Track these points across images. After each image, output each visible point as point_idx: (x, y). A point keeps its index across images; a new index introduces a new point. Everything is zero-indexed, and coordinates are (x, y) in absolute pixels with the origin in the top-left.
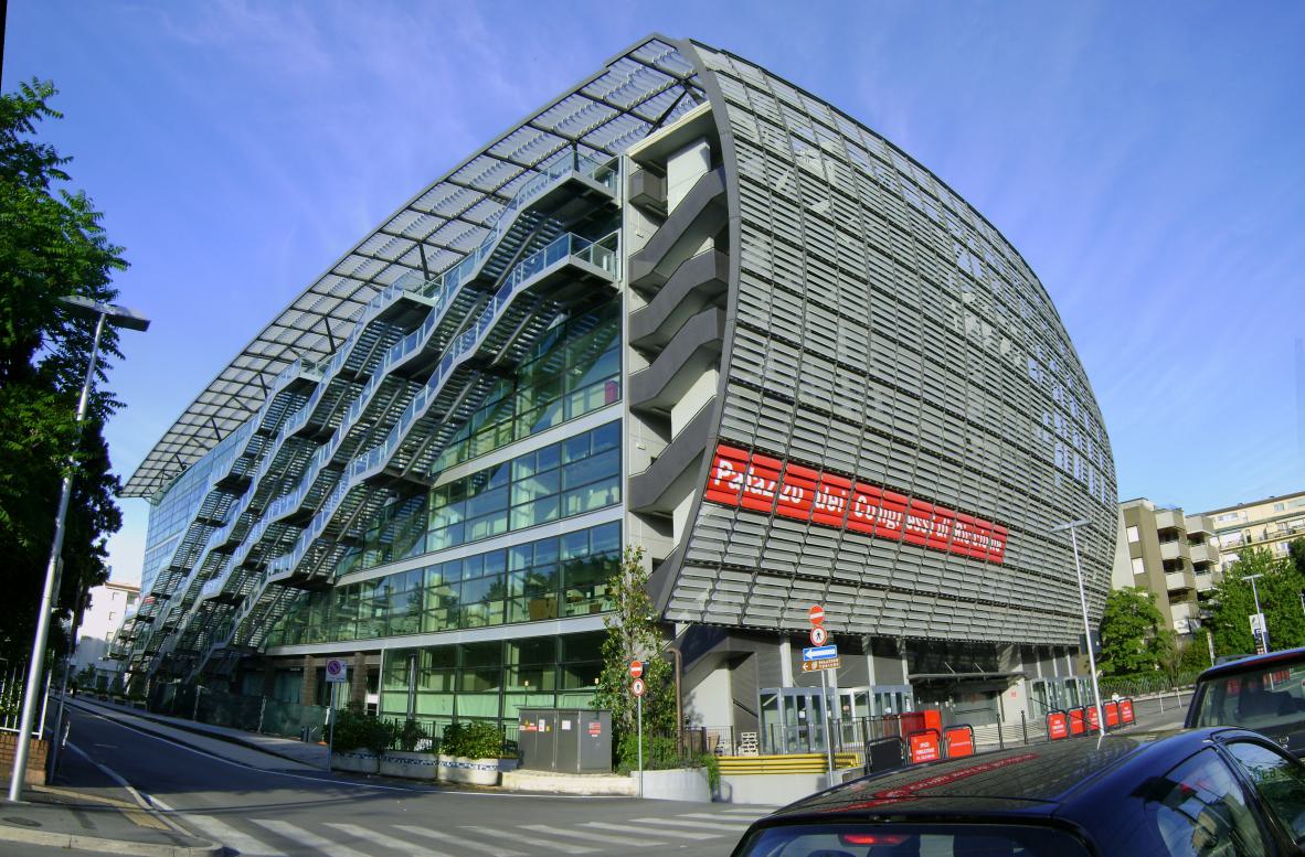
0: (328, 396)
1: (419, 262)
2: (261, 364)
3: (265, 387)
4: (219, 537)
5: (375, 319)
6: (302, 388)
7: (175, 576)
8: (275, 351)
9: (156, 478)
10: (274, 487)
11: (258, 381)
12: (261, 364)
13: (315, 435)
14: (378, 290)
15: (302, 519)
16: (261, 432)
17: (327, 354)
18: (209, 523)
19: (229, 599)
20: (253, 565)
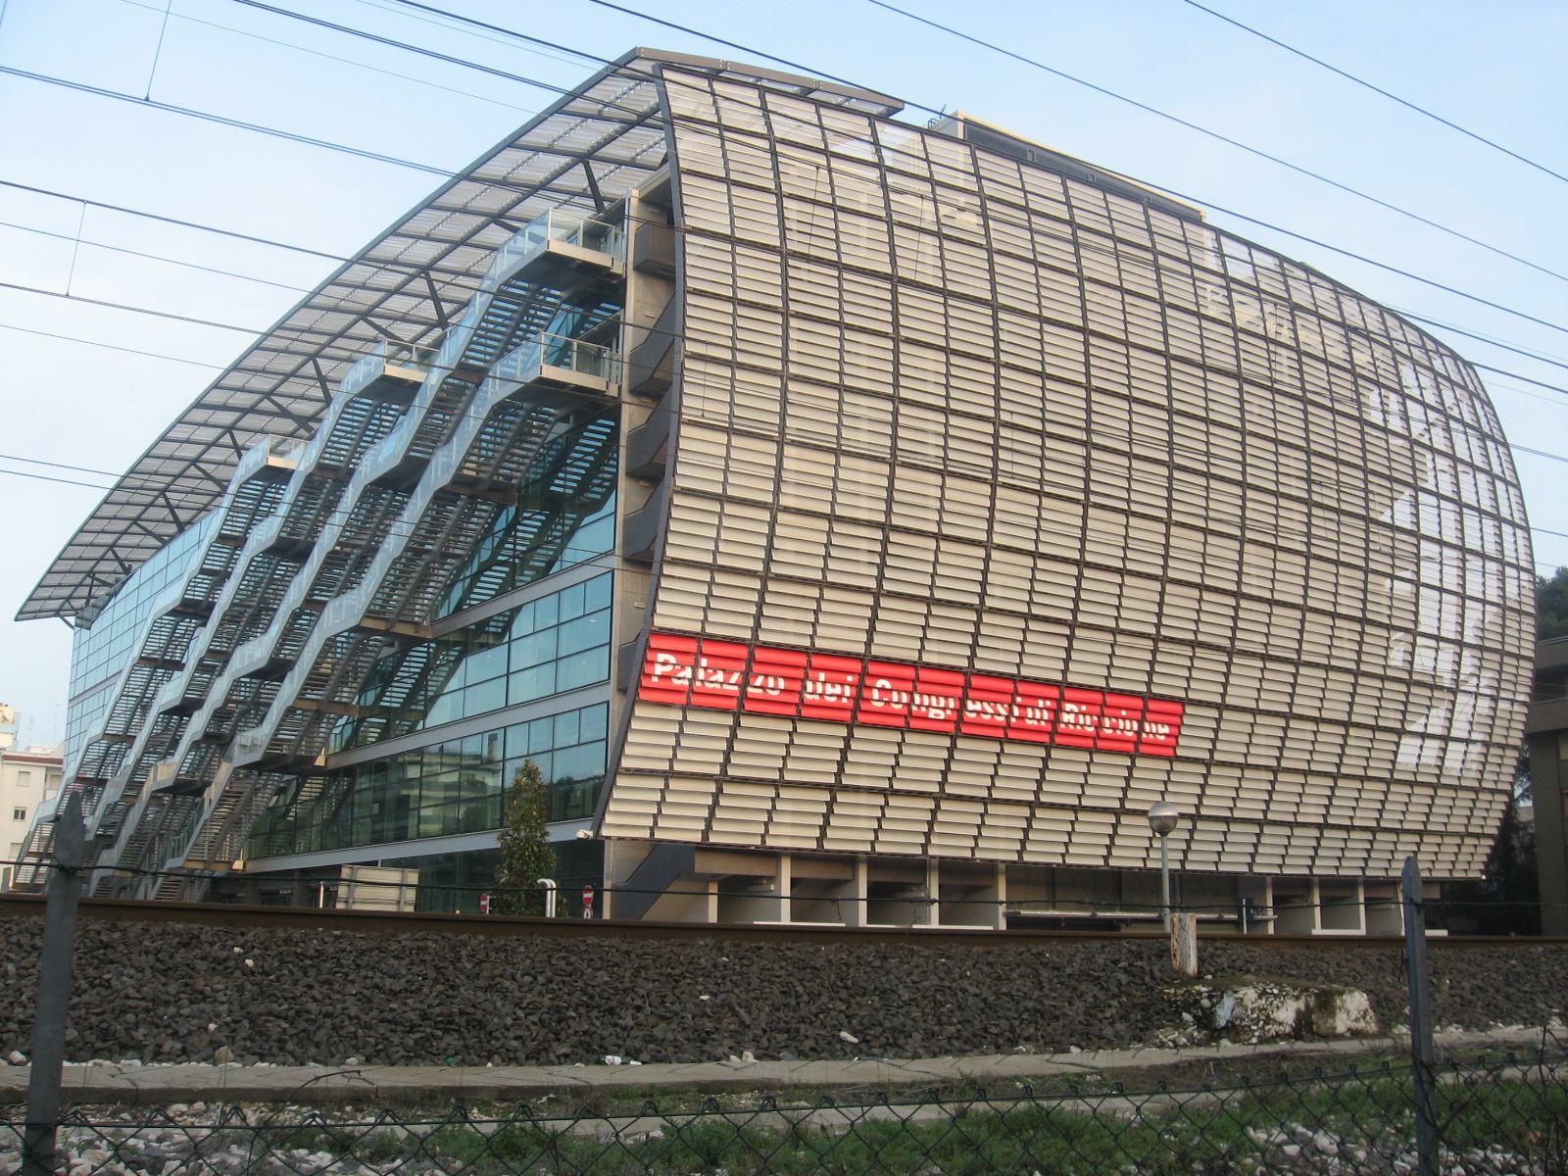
0: (440, 404)
1: (426, 290)
2: (227, 418)
3: (322, 379)
4: (171, 692)
5: (513, 278)
6: (392, 393)
7: (115, 748)
8: (246, 400)
9: (80, 585)
10: (249, 617)
11: (227, 440)
12: (227, 418)
13: (290, 550)
14: (515, 230)
15: (275, 670)
16: (222, 538)
17: (432, 326)
18: (160, 663)
19: (187, 789)
20: (216, 741)
